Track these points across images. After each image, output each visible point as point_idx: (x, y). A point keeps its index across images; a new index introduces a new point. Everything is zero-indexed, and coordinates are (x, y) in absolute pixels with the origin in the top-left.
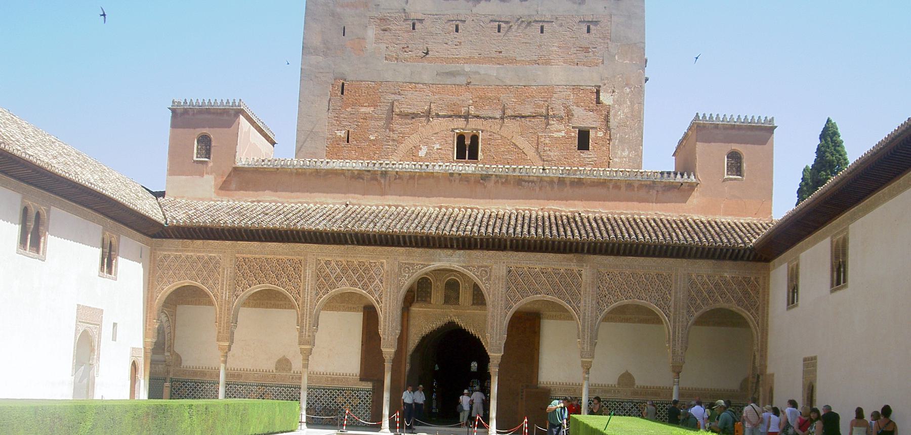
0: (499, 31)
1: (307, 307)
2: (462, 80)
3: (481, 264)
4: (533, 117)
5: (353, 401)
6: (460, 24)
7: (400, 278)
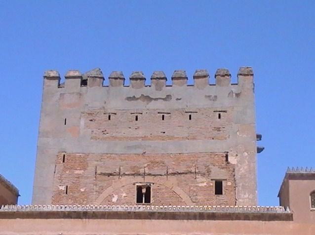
0: (163, 119)
2: (140, 151)
4: (186, 173)
6: (139, 116)
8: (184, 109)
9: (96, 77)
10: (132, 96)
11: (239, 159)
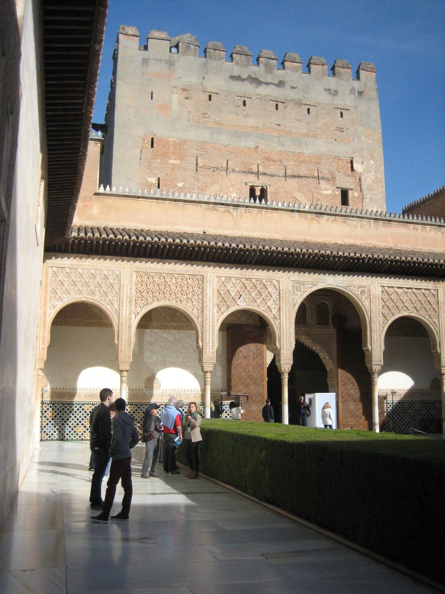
0: (277, 108)
1: (209, 324)
2: (251, 144)
3: (360, 284)
4: (308, 177)
7: (293, 297)
8: (301, 100)
9: (191, 44)
10: (237, 75)
11: (365, 167)
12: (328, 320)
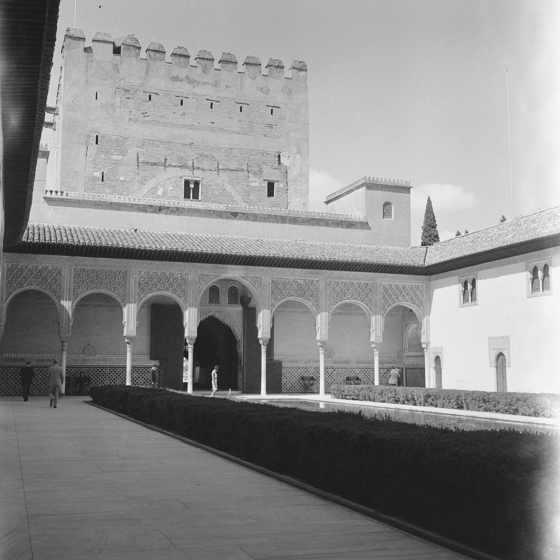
0: (212, 108)
3: (254, 276)
4: (238, 170)
5: (145, 375)
8: (235, 99)
12: (237, 300)
